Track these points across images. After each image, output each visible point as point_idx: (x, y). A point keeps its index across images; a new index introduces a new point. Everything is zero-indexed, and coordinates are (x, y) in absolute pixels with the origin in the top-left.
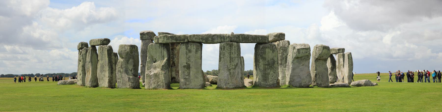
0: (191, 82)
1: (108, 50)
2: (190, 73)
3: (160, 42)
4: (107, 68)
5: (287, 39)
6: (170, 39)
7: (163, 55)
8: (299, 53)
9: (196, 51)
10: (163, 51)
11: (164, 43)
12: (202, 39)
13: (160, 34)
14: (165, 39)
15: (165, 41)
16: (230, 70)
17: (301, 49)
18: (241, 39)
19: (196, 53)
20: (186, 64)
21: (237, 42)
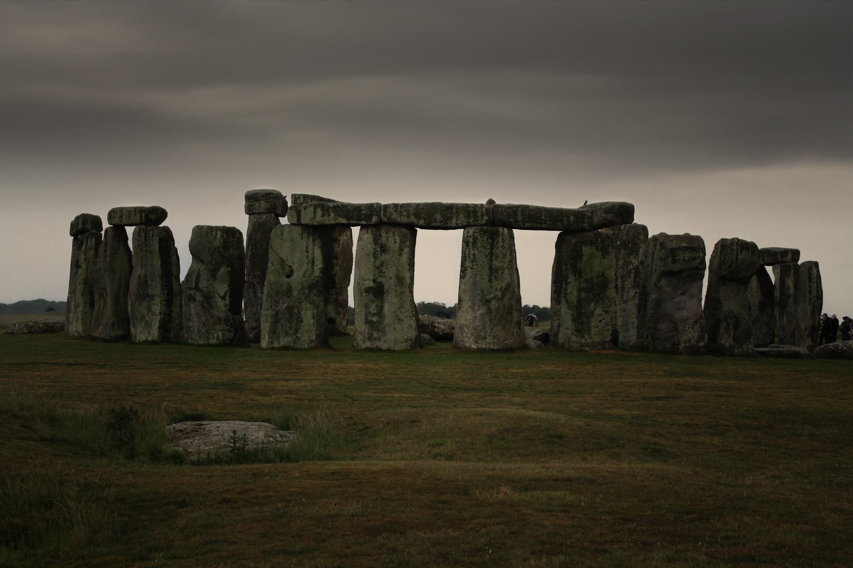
0: (384, 333)
2: (382, 308)
3: (303, 222)
4: (156, 290)
5: (638, 220)
6: (332, 215)
9: (401, 249)
10: (310, 246)
11: (316, 224)
12: (417, 215)
13: (295, 197)
15: (319, 219)
16: (488, 301)
17: (680, 248)
18: (520, 218)
20: (372, 284)
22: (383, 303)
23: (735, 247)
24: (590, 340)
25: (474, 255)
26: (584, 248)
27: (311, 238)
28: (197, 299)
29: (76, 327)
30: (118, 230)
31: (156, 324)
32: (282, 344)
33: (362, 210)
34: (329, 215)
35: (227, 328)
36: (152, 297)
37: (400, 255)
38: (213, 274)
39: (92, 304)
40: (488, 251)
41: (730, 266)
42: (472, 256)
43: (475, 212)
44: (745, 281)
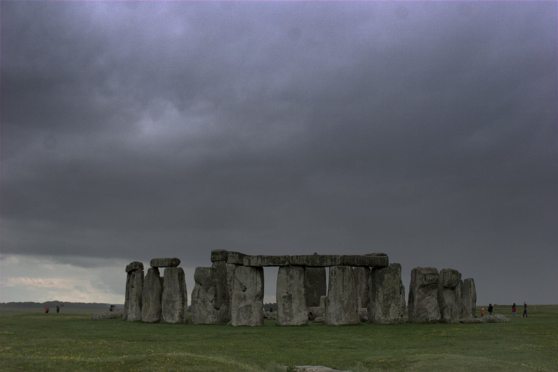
0: (292, 317)
1: (179, 274)
2: (291, 306)
3: (252, 265)
6: (266, 261)
8: (425, 279)
12: (307, 260)
14: (260, 261)
18: (356, 262)
20: (286, 295)
22: (291, 302)
24: (389, 319)
29: (132, 316)
30: (155, 270)
31: (177, 315)
32: (242, 324)
36: (175, 302)
37: (300, 280)
38: (207, 290)
39: (141, 305)
43: (335, 259)
44: (453, 289)
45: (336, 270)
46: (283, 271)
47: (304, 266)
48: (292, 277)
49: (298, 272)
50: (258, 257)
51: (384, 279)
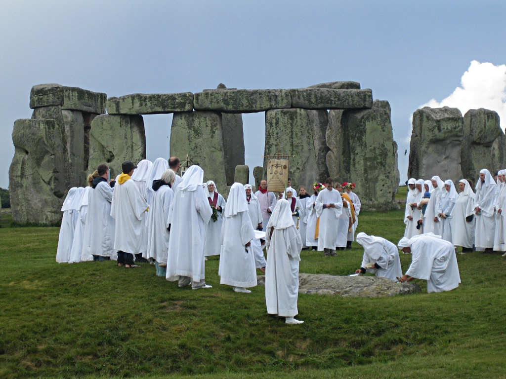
3: (122, 112)
6: (149, 104)
7: (130, 144)
8: (439, 130)
11: (134, 113)
12: (226, 101)
17: (443, 120)
18: (313, 100)
19: (212, 137)
21: (306, 109)
23: (482, 116)
24: (376, 202)
25: (277, 134)
26: (367, 123)
27: (129, 126)
28: (24, 185)
33: (175, 99)
34: (146, 105)
35: (54, 210)
37: (212, 137)
38: (38, 162)
40: (289, 130)
41: (481, 132)
42: (275, 134)
44: (488, 145)
45: (279, 116)
46: (182, 121)
47: (219, 112)
48: (197, 133)
49: (209, 123)
50: (133, 97)
51: (365, 132)
